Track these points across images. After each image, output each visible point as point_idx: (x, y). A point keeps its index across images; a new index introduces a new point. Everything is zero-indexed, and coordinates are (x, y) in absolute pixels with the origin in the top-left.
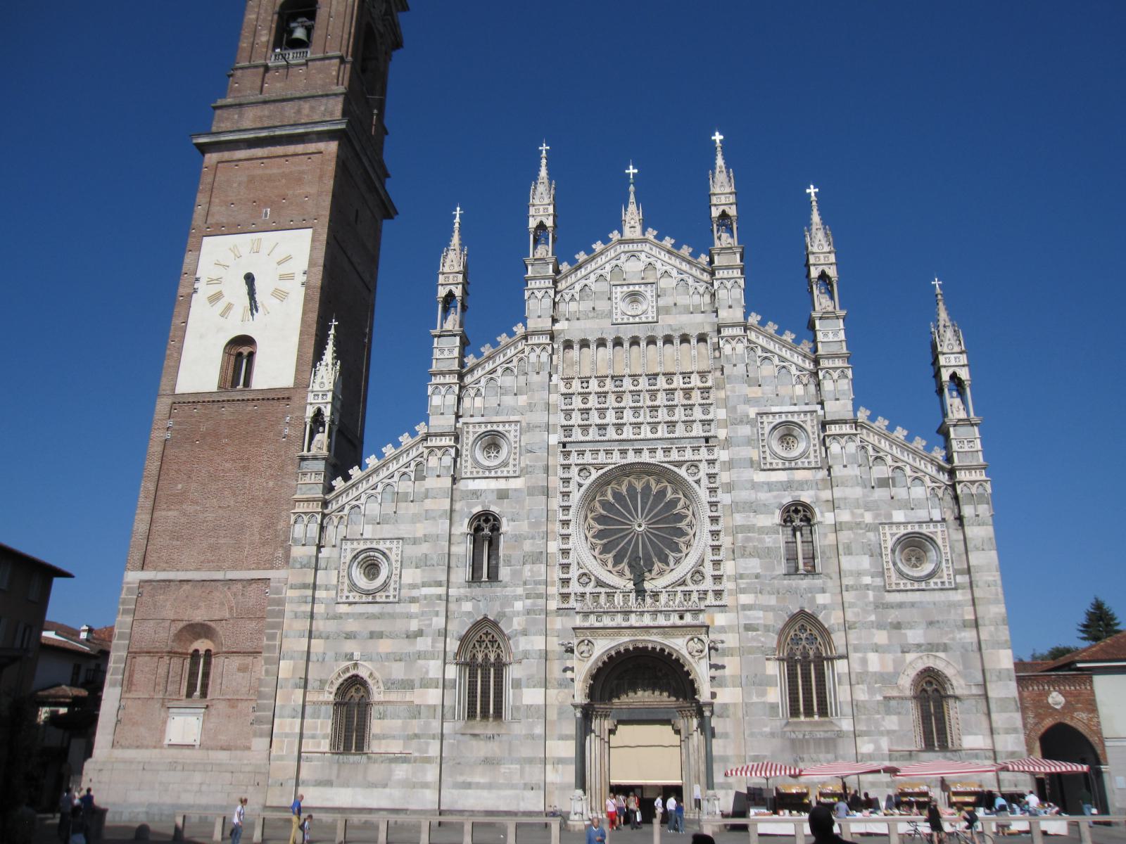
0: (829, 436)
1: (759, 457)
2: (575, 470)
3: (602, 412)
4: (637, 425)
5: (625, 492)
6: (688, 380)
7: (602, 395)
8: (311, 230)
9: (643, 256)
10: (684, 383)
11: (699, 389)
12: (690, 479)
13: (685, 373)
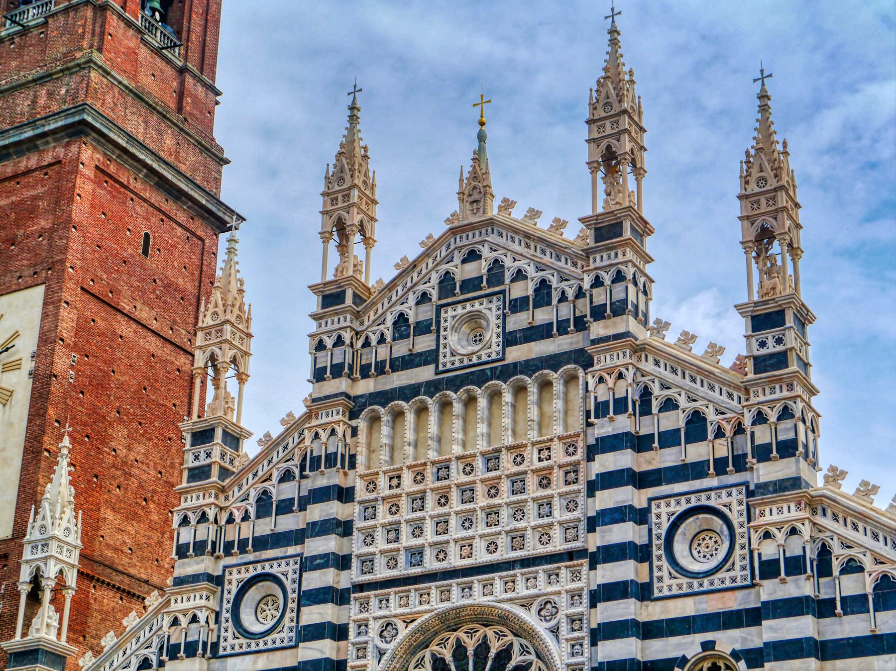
0: (756, 529)
1: (651, 577)
2: (374, 628)
3: (418, 530)
4: (467, 545)
5: (448, 656)
6: (546, 453)
7: (418, 500)
8: (43, 287)
9: (485, 251)
10: (540, 460)
11: (560, 467)
12: (541, 628)
13: (540, 442)
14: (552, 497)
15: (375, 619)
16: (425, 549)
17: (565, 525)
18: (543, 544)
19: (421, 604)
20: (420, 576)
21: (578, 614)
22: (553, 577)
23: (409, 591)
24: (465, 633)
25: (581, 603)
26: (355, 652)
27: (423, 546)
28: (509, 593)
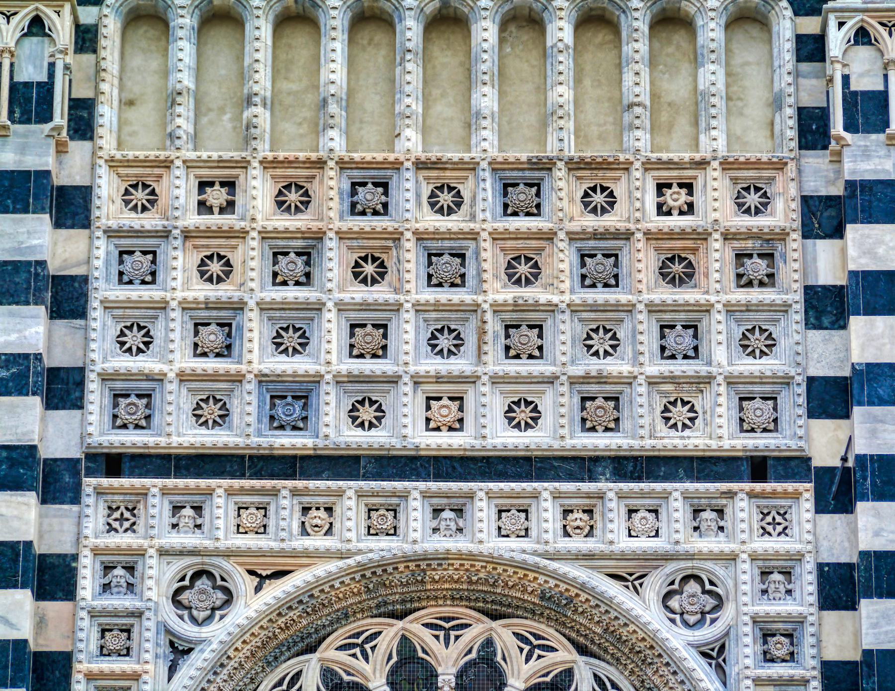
6: (683, 197)
10: (662, 210)
11: (727, 237)
13: (670, 164)
14: (707, 309)
15: (163, 553)
16: (324, 388)
17: (741, 387)
18: (674, 426)
19: (304, 532)
20: (304, 458)
21: (788, 619)
22: (708, 515)
23: (275, 493)
24: (426, 625)
25: (789, 592)
26: (95, 634)
27: (316, 380)
28: (575, 538)
